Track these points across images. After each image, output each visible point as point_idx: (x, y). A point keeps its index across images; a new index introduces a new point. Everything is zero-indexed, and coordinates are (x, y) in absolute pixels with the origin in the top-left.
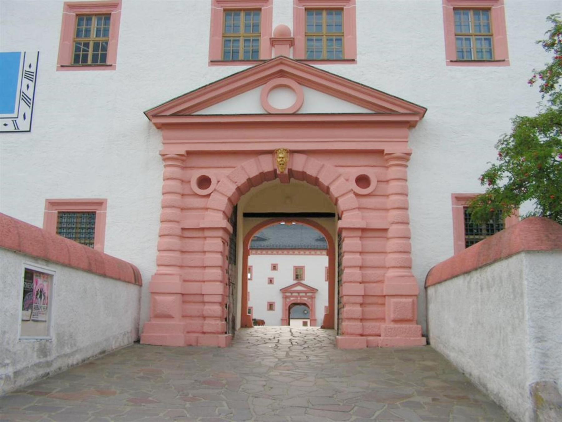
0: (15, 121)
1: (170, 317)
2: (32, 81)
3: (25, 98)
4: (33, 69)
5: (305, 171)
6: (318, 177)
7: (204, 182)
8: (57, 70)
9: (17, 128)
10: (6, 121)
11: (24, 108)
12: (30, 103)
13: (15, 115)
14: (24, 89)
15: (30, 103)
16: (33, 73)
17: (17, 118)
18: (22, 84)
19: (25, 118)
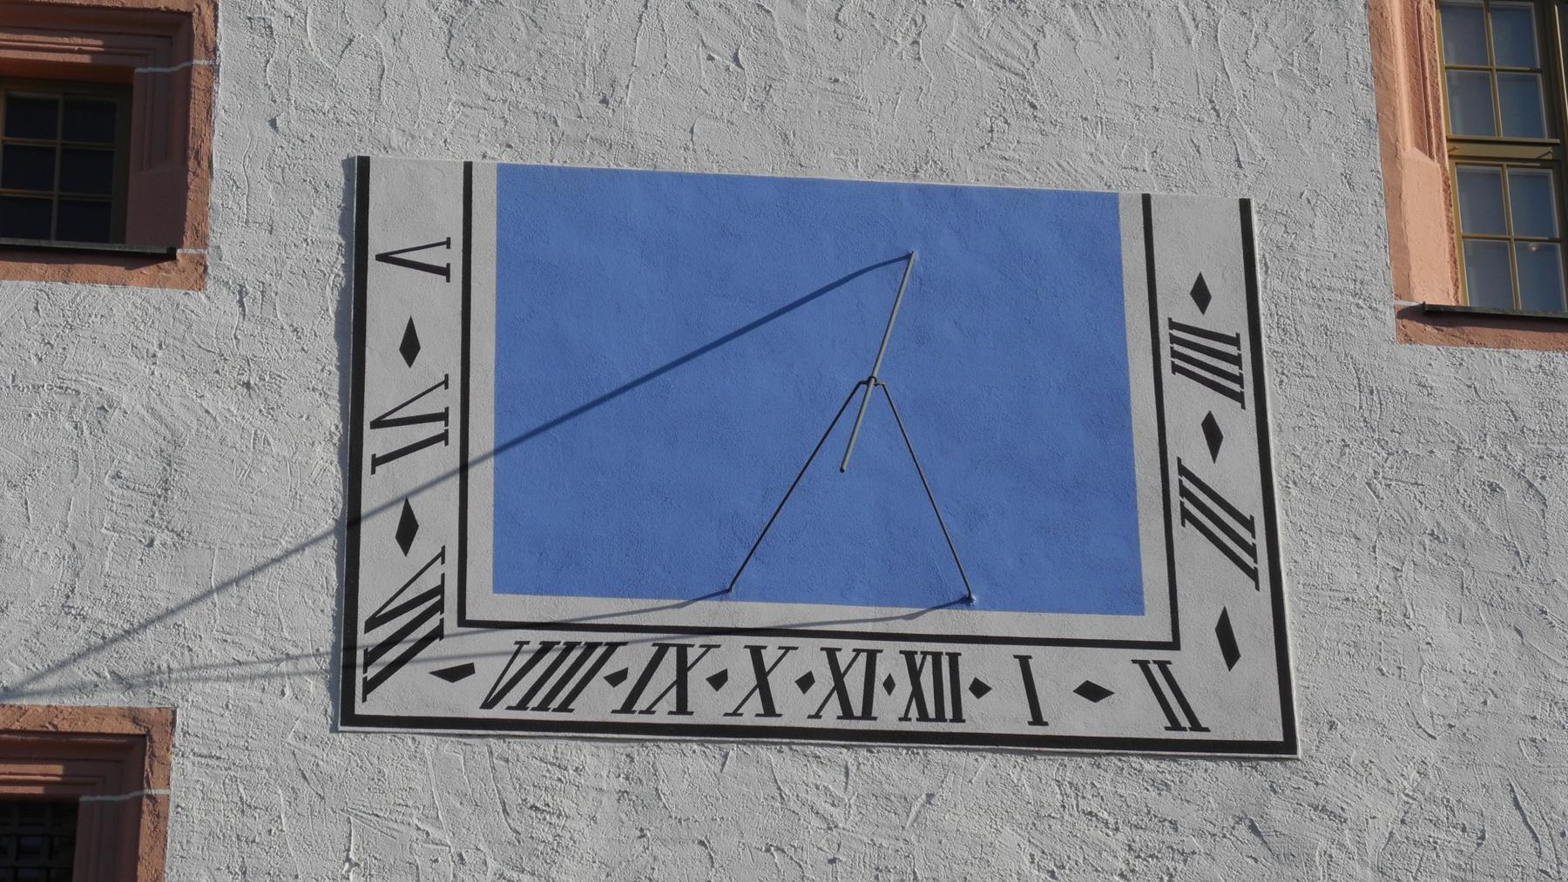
0: (1163, 665)
2: (1239, 397)
4: (1226, 315)
12: (1251, 551)
15: (1251, 551)
16: (1235, 341)
17: (1174, 645)
19: (1231, 653)
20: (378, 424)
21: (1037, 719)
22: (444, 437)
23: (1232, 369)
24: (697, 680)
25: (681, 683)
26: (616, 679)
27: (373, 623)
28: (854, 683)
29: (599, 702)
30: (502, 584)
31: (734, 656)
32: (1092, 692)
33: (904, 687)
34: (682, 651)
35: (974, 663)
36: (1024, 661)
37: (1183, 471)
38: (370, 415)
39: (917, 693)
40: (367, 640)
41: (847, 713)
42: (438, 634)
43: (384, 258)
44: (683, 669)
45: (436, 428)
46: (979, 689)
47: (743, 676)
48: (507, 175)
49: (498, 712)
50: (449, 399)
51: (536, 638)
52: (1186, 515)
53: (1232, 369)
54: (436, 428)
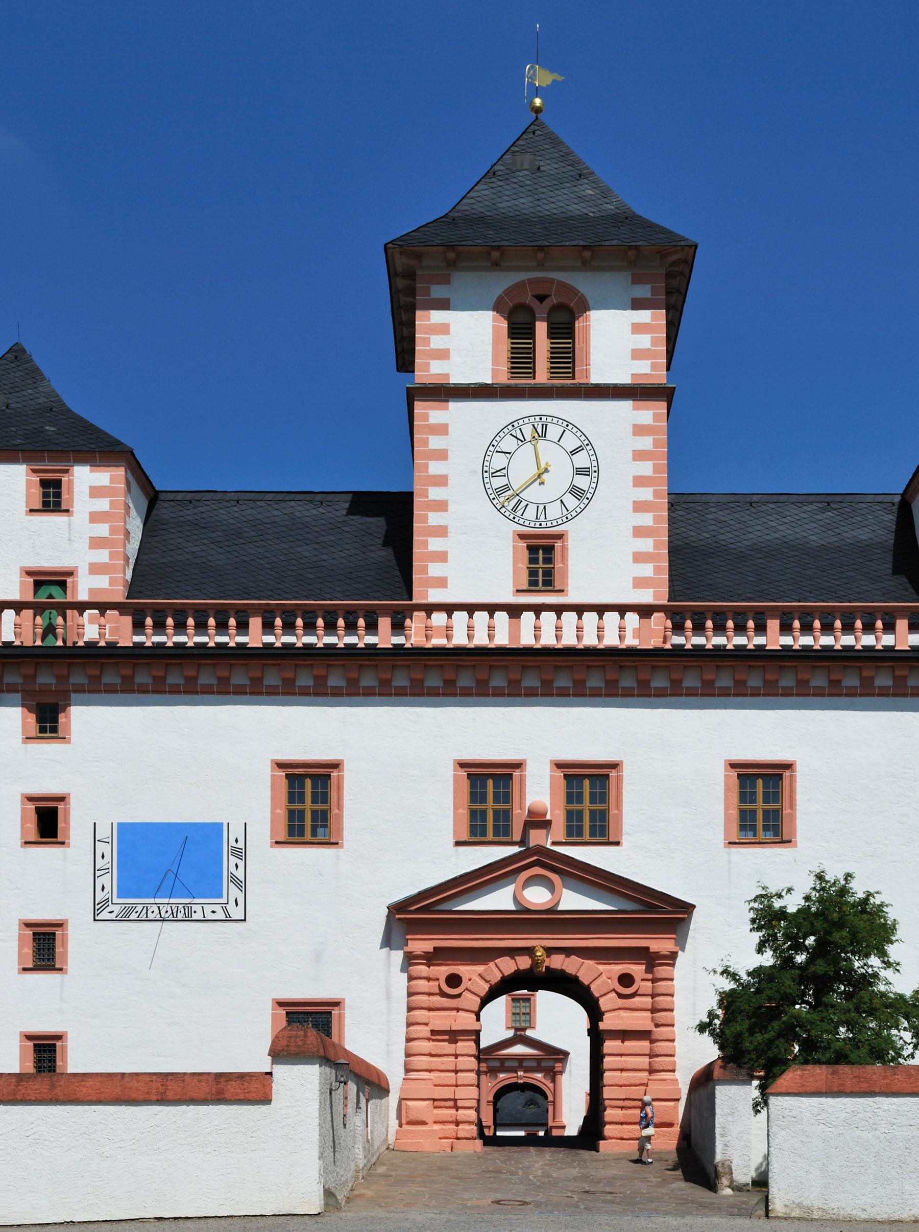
1: (424, 1123)
2: (242, 859)
3: (234, 880)
4: (241, 844)
5: (564, 968)
6: (577, 975)
7: (454, 980)
8: (271, 847)
9: (228, 916)
10: (214, 907)
11: (235, 892)
12: (242, 887)
13: (224, 900)
14: (232, 869)
15: (242, 887)
16: (242, 849)
17: (227, 904)
18: (229, 863)
19: (237, 905)
20: (98, 870)
21: (204, 917)
22: (108, 872)
23: (241, 854)
24: (149, 912)
25: (147, 913)
26: (137, 912)
27: (98, 904)
28: (175, 911)
29: (134, 916)
30: (118, 897)
31: (155, 908)
32: (214, 912)
33: (183, 912)
34: (147, 907)
35: (194, 908)
36: (203, 907)
37: (231, 873)
38: (96, 869)
39: (185, 913)
40: (97, 907)
41: (173, 917)
42: (108, 905)
43: (98, 841)
44: (147, 910)
45: (107, 871)
46: (195, 912)
47: (157, 911)
48: (119, 825)
49: (118, 918)
50: (109, 866)
51: (124, 906)
52: (231, 881)
53: (241, 854)
54: (107, 871)
